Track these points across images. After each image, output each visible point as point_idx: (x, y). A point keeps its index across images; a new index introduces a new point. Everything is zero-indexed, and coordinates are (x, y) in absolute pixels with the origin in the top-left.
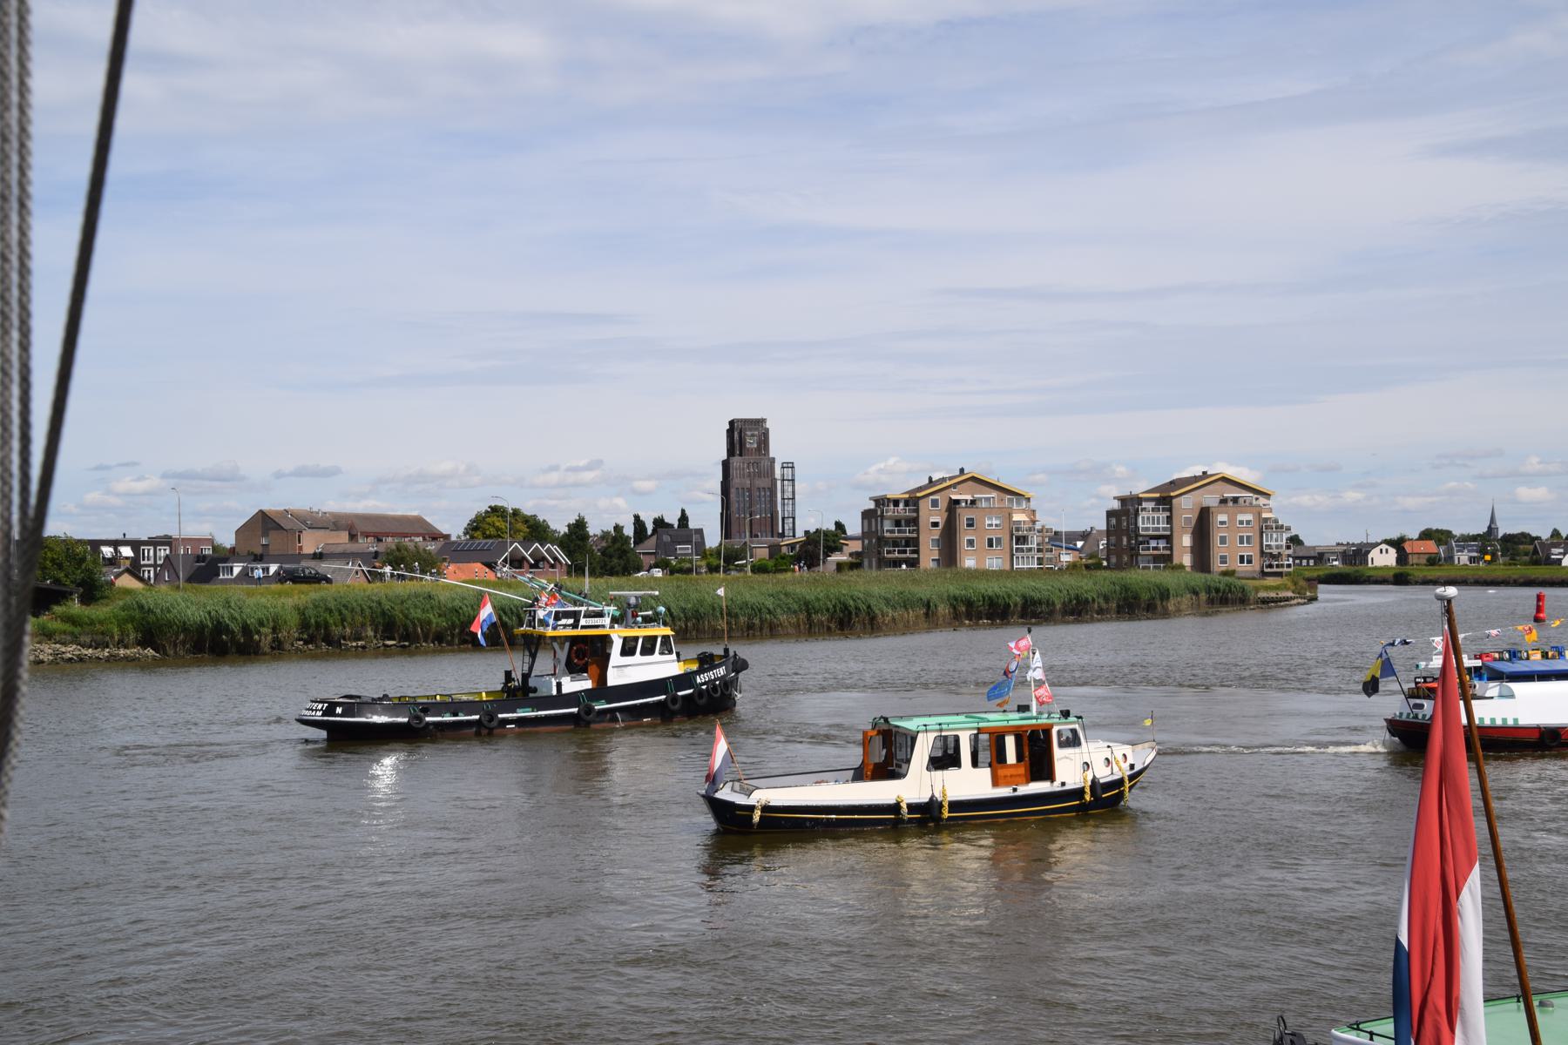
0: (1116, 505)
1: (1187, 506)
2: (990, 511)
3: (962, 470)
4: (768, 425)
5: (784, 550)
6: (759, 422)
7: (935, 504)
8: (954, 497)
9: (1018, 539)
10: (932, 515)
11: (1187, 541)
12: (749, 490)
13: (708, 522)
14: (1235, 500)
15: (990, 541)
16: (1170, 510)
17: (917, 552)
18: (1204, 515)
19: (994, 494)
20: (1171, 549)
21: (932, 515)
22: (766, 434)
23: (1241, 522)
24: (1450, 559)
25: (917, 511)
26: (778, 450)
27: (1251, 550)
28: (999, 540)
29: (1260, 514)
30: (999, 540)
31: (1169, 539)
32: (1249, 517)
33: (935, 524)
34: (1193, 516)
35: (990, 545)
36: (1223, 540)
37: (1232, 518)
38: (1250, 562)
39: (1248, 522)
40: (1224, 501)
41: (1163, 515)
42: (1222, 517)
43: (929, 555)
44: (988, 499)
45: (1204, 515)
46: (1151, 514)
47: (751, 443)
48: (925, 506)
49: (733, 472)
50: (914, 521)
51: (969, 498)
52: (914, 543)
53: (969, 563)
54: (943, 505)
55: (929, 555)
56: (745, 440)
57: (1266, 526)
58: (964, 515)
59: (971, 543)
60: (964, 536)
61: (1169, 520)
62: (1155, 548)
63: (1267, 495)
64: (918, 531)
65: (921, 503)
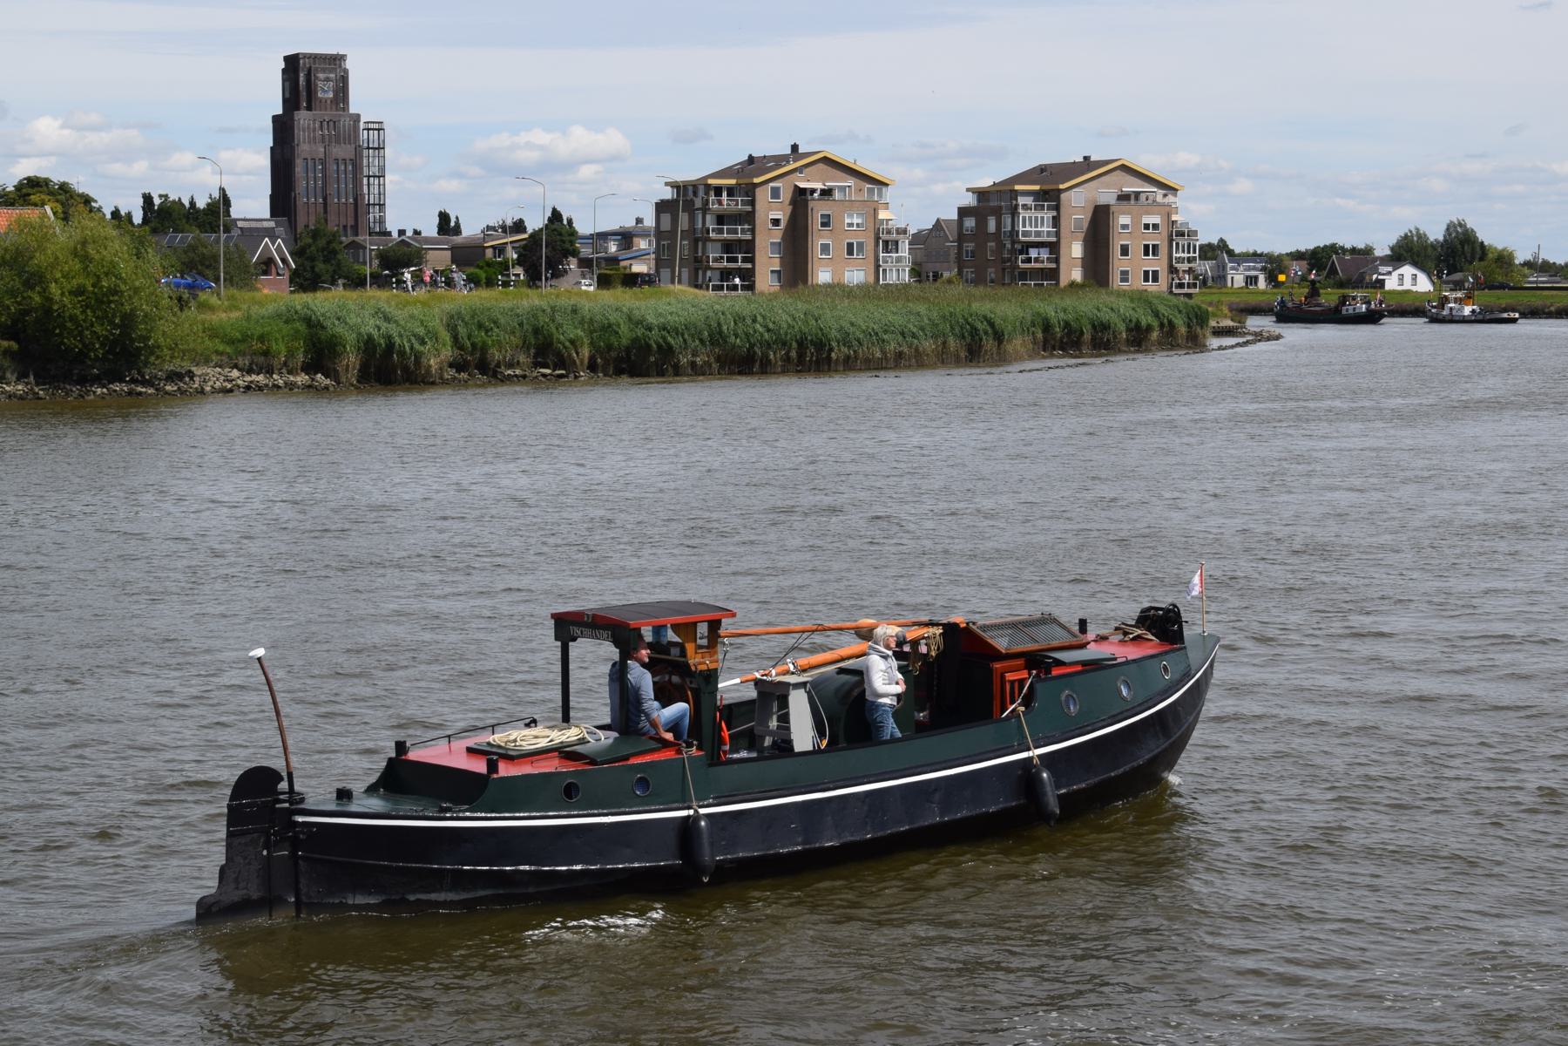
0: (668, 194)
1: (1078, 201)
2: (851, 205)
3: (795, 148)
4: (349, 64)
5: (489, 253)
6: (336, 60)
7: (775, 193)
8: (802, 185)
9: (886, 243)
10: (772, 210)
11: (1077, 250)
12: (323, 162)
13: (252, 203)
14: (1137, 194)
15: (850, 246)
16: (1057, 208)
17: (752, 260)
18: (1100, 218)
19: (850, 182)
20: (1057, 261)
21: (772, 210)
22: (344, 80)
23: (1147, 226)
24: (1220, 278)
25: (753, 203)
26: (361, 102)
27: (1158, 264)
28: (860, 245)
29: (1169, 216)
30: (860, 245)
31: (1054, 248)
32: (1156, 219)
33: (776, 222)
34: (1084, 217)
35: (850, 252)
36: (1125, 250)
37: (1136, 220)
38: (1155, 279)
39: (1155, 226)
40: (1123, 198)
41: (1048, 215)
42: (1124, 220)
43: (767, 264)
44: (842, 189)
45: (1100, 218)
46: (1033, 214)
47: (325, 92)
48: (763, 196)
49: (300, 135)
50: (749, 218)
51: (819, 186)
52: (749, 247)
53: (823, 276)
54: (786, 195)
55: (767, 264)
56: (309, 83)
57: (1178, 234)
58: (818, 209)
59: (825, 248)
60: (819, 239)
61: (1056, 221)
62: (1037, 260)
63: (1174, 190)
64: (753, 231)
65: (758, 191)
